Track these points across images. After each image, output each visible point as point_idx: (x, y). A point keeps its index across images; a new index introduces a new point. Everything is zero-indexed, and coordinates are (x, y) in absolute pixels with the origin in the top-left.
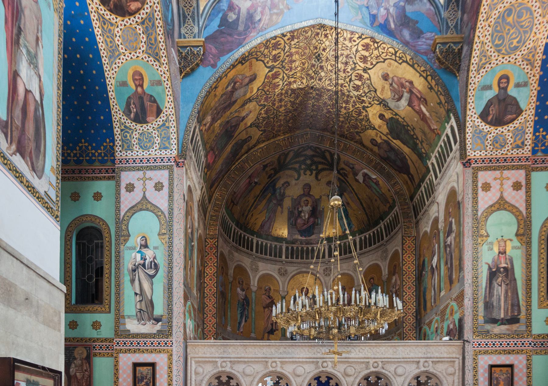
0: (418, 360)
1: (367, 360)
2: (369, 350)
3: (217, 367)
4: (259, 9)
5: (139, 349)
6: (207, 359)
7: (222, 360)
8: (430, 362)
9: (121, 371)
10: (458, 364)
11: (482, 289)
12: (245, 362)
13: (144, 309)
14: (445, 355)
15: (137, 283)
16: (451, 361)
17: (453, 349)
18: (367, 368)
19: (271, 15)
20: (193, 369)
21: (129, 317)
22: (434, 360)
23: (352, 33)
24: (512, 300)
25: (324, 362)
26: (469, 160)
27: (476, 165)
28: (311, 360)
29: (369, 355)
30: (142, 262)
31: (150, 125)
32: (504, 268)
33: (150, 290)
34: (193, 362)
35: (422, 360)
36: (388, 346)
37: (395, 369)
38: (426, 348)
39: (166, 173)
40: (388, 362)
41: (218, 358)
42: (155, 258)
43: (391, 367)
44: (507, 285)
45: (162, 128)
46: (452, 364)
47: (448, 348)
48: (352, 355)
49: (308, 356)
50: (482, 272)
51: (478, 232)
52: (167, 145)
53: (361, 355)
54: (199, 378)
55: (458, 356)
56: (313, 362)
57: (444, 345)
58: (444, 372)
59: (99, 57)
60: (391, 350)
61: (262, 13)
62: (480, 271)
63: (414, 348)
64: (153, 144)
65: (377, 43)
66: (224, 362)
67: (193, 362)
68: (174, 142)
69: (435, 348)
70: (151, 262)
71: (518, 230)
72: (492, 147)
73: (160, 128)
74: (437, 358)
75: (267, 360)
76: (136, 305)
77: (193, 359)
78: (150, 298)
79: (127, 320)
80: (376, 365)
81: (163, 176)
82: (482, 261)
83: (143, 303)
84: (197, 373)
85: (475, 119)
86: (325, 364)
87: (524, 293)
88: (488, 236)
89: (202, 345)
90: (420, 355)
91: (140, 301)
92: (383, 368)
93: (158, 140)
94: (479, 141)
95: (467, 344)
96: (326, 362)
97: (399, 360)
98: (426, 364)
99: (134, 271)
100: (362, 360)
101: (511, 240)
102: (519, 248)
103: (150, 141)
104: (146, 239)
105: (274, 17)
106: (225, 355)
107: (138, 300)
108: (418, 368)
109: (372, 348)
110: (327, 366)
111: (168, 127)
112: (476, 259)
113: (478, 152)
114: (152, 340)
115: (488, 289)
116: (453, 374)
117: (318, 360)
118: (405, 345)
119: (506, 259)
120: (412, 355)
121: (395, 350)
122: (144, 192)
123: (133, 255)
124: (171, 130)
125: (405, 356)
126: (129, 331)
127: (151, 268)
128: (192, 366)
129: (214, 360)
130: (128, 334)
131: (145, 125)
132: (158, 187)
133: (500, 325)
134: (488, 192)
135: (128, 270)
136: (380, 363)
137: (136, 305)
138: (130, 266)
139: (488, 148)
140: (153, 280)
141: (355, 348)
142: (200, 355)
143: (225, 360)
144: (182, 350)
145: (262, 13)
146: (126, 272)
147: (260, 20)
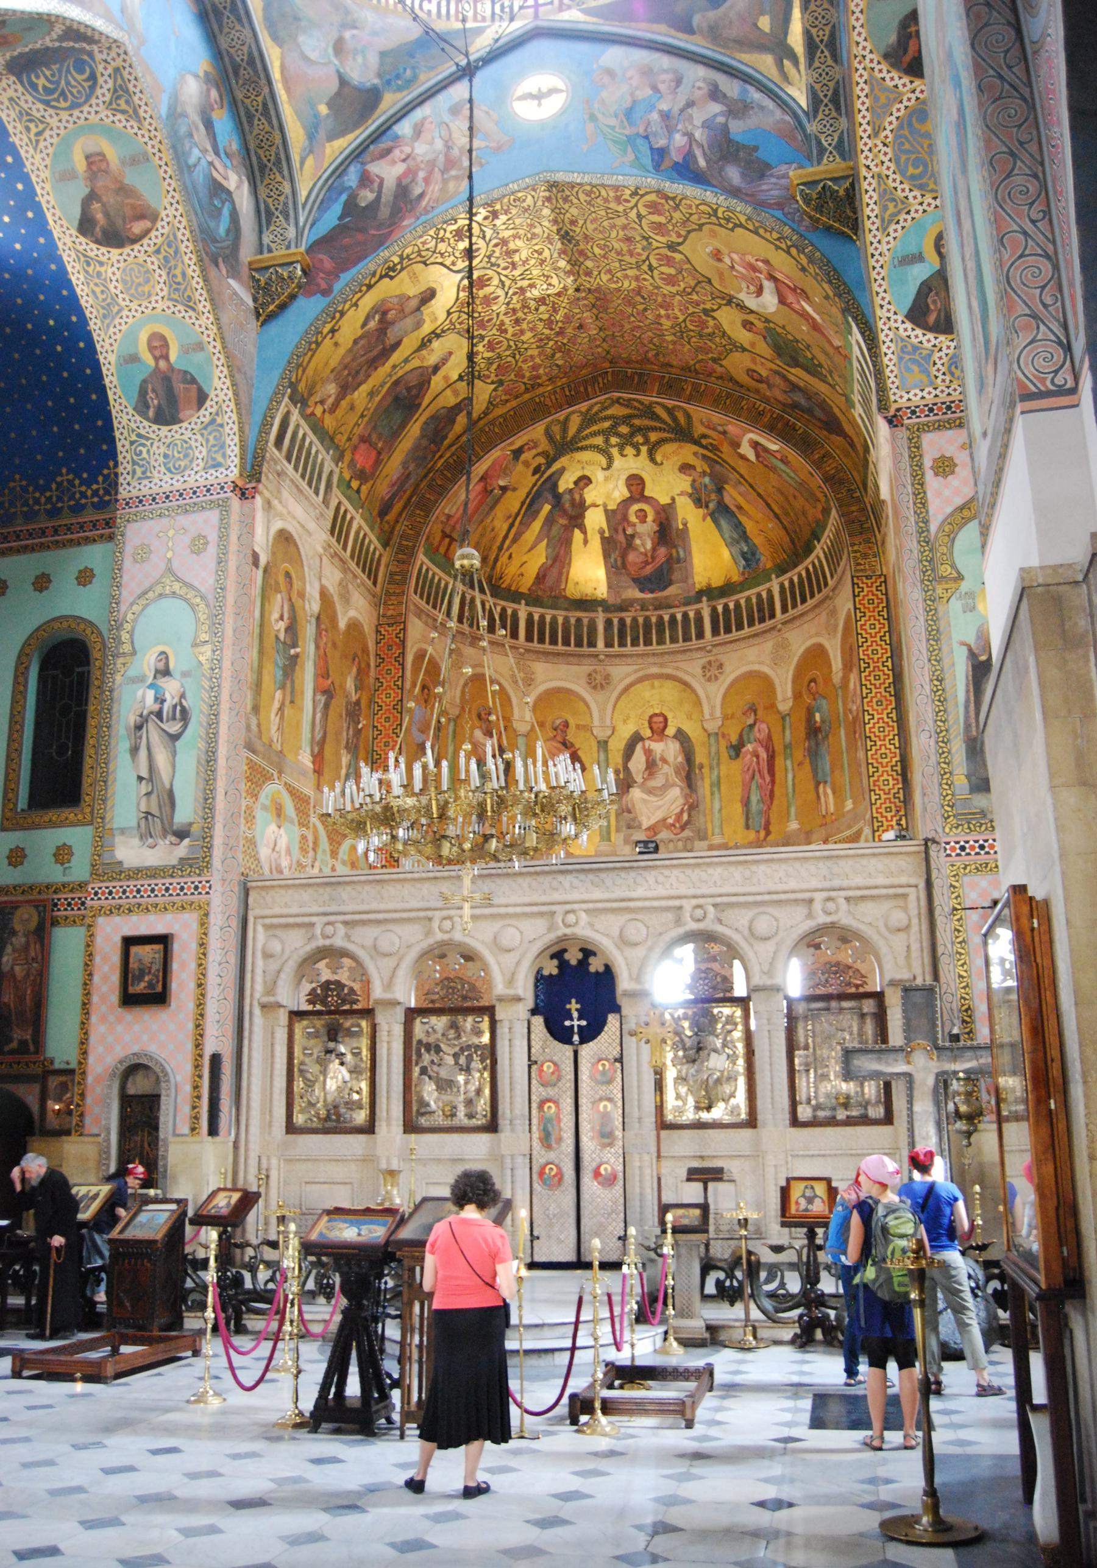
0: (807, 895)
1: (677, 903)
2: (682, 877)
3: (313, 937)
4: (421, 175)
5: (140, 905)
6: (291, 920)
7: (325, 919)
8: (842, 901)
9: (98, 959)
10: (916, 898)
12: (378, 922)
13: (155, 810)
14: (881, 880)
15: (143, 753)
16: (896, 896)
17: (902, 863)
18: (678, 922)
19: (445, 182)
20: (259, 946)
21: (123, 831)
22: (851, 893)
23: (616, 188)
25: (568, 912)
26: (898, 410)
27: (915, 420)
28: (535, 909)
29: (683, 891)
30: (156, 707)
31: (185, 425)
33: (170, 769)
34: (260, 929)
35: (819, 897)
36: (729, 863)
37: (751, 922)
38: (829, 863)
39: (213, 516)
40: (731, 905)
41: (318, 915)
42: (183, 696)
43: (741, 919)
45: (209, 429)
46: (901, 903)
47: (887, 860)
48: (640, 892)
49: (527, 900)
51: (933, 570)
52: (220, 459)
53: (661, 891)
54: (274, 966)
55: (913, 881)
56: (541, 914)
57: (874, 855)
58: (881, 924)
59: (83, 320)
60: (737, 873)
61: (427, 180)
63: (797, 865)
64: (191, 461)
65: (673, 199)
66: (328, 924)
67: (260, 929)
68: (233, 451)
69: (850, 862)
70: (175, 707)
72: (948, 378)
73: (205, 428)
74: (859, 888)
75: (429, 914)
76: (138, 805)
77: (260, 921)
78: (168, 786)
79: (118, 839)
80: (699, 913)
81: (207, 522)
83: (154, 797)
84: (267, 955)
85: (899, 324)
86: (571, 918)
88: (960, 577)
89: (280, 886)
90: (814, 883)
91: (148, 794)
92: (720, 921)
93: (201, 452)
94: (915, 368)
95: (933, 848)
96: (573, 911)
97: (759, 898)
98: (831, 906)
99: (139, 727)
100: (664, 903)
103: (186, 456)
104: (167, 658)
105: (452, 185)
106: (333, 908)
107: (144, 792)
108: (810, 915)
109: (689, 871)
110: (577, 923)
111: (221, 426)
112: (934, 635)
113: (917, 391)
114: (167, 881)
115: (972, 705)
116: (907, 928)
117: (554, 908)
118: (772, 860)
120: (793, 885)
121: (747, 873)
122: (170, 560)
123: (140, 693)
124: (227, 429)
125: (773, 888)
126: (120, 863)
127: (174, 718)
128: (258, 936)
129: (306, 920)
130: (118, 871)
131: (175, 427)
132: (198, 545)
134: (950, 478)
135: (127, 729)
136: (711, 909)
137: (138, 805)
138: (132, 719)
139: (939, 380)
140: (178, 744)
141: (645, 874)
142: (277, 910)
143: (332, 918)
144: (235, 903)
145: (427, 180)
146: (122, 732)
147: (422, 196)
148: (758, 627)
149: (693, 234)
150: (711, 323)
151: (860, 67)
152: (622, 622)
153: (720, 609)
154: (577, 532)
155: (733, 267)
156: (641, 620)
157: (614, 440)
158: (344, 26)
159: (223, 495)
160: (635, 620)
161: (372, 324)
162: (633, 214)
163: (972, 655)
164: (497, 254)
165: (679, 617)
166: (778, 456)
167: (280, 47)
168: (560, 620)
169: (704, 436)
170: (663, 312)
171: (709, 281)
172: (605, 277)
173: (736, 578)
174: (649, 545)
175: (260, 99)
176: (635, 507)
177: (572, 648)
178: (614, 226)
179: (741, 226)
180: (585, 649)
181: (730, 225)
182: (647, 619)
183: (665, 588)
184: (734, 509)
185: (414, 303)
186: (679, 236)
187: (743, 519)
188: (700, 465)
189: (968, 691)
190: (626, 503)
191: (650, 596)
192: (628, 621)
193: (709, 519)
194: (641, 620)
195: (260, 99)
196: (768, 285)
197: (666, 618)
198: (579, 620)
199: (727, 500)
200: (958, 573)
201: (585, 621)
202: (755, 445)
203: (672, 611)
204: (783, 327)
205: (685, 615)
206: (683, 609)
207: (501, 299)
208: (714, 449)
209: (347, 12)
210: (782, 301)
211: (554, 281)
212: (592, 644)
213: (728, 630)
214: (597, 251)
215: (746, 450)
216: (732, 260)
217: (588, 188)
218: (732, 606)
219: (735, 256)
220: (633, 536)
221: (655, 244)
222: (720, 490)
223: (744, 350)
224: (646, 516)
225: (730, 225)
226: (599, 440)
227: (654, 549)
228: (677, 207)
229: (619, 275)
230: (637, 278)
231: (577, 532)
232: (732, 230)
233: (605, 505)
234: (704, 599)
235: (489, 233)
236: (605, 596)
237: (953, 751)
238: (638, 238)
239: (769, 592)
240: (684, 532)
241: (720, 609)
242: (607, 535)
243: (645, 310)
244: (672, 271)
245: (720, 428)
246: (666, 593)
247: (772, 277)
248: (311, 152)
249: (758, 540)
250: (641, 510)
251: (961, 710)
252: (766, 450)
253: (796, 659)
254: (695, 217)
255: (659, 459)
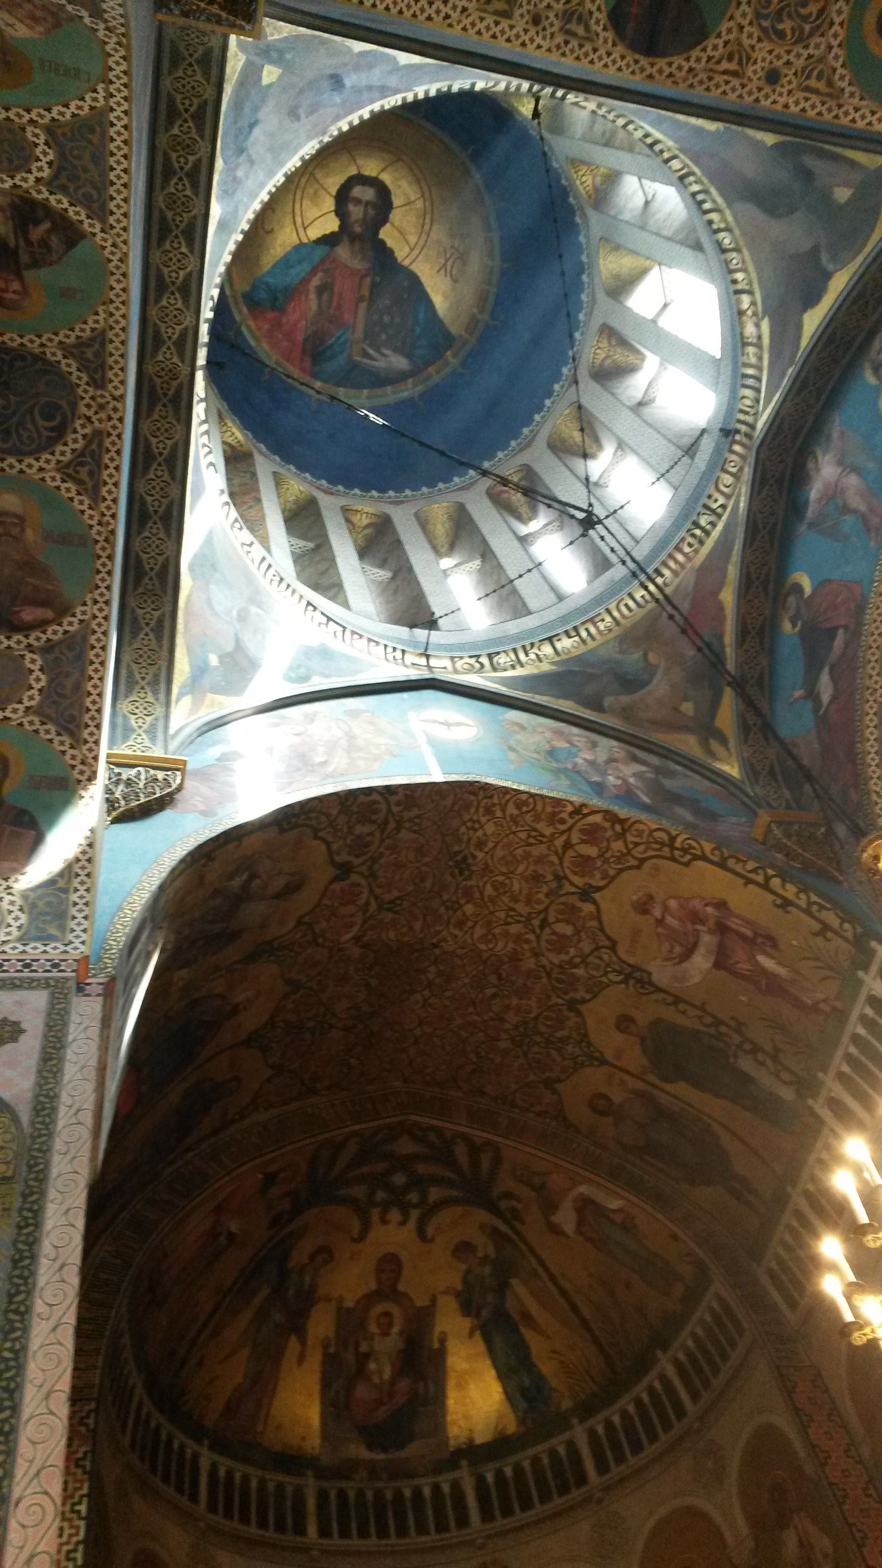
148: (558, 1502)
149: (625, 875)
150: (573, 1020)
151: (871, 699)
152: (342, 1495)
153: (490, 1478)
154: (293, 1339)
155: (660, 922)
156: (370, 1495)
157: (380, 1195)
158: (252, 601)
159: (55, 974)
160: (361, 1494)
161: (237, 883)
162: (559, 842)
164: (382, 861)
165: (427, 1491)
166: (619, 1218)
167: (193, 580)
168: (254, 1483)
169: (509, 1195)
170: (515, 1001)
171: (613, 947)
172: (479, 932)
173: (512, 1427)
174: (387, 1373)
175: (156, 614)
176: (379, 1308)
177: (270, 1534)
178: (528, 855)
179: (704, 858)
180: (289, 1538)
181: (688, 857)
182: (379, 1495)
183: (402, 1446)
184: (516, 1316)
185: (279, 883)
186: (605, 875)
187: (528, 1334)
188: (485, 1246)
190: (369, 1299)
191: (381, 1456)
192: (352, 1494)
193: (478, 1335)
194: (370, 1495)
195: (156, 614)
196: (708, 940)
197: (408, 1493)
198: (280, 1486)
199: (510, 1304)
201: (289, 1489)
202: (585, 1205)
203: (416, 1482)
204: (702, 1008)
205: (436, 1488)
206: (431, 1480)
207: (355, 929)
208: (514, 1217)
209: (257, 591)
210: (721, 962)
211: (418, 926)
212: (300, 1529)
213: (507, 1512)
214: (489, 890)
215: (566, 1218)
216: (666, 909)
217: (524, 797)
218: (508, 1471)
219: (673, 904)
220: (367, 1356)
221: (568, 888)
222: (502, 1288)
223: (603, 1062)
224: (390, 1325)
225: (688, 857)
226: (359, 1192)
227: (393, 1381)
228: (621, 836)
229: (497, 931)
230: (518, 939)
231: (293, 1339)
232: (687, 864)
233: (341, 1299)
234: (464, 1463)
235: (392, 825)
236: (317, 1451)
238: (549, 877)
239: (571, 1445)
240: (439, 1357)
241: (490, 1478)
242: (332, 1350)
243: (494, 996)
244: (568, 930)
245: (537, 1181)
246: (403, 1454)
247: (721, 929)
248: (192, 692)
249: (547, 1367)
250: (387, 1314)
252: (600, 1211)
253: (640, 1545)
254: (641, 848)
255: (430, 1231)
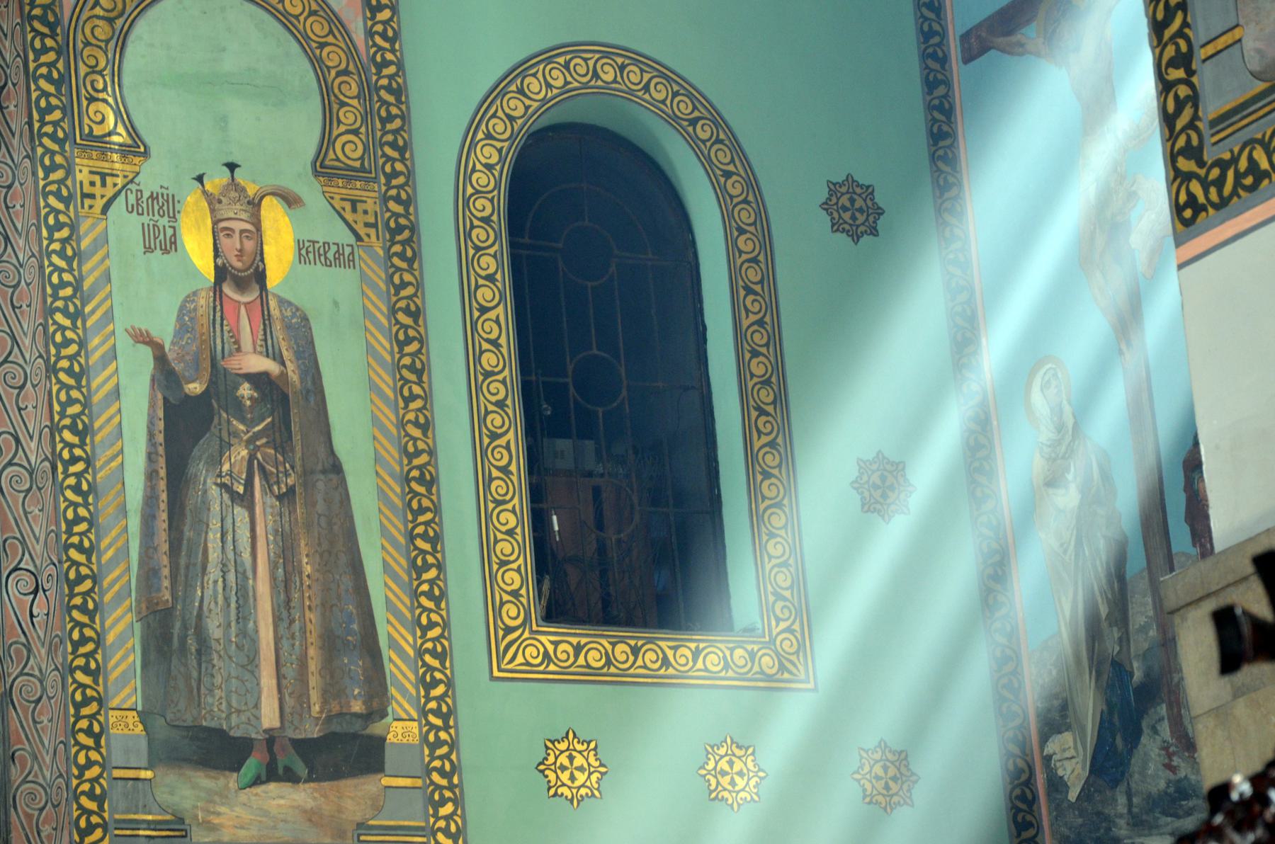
11: (122, 510)
24: (326, 607)
32: (259, 380)
44: (287, 497)
50: (116, 393)
51: (66, 110)
62: (100, 383)
71: (327, 141)
82: (109, 317)
87: (400, 564)
88: (136, 148)
101: (290, 200)
102: (341, 259)
119: (267, 319)
133: (257, 781)
163: (165, 375)
189: (151, 475)
200: (133, 131)
237: (110, 638)
251: (134, 523)
